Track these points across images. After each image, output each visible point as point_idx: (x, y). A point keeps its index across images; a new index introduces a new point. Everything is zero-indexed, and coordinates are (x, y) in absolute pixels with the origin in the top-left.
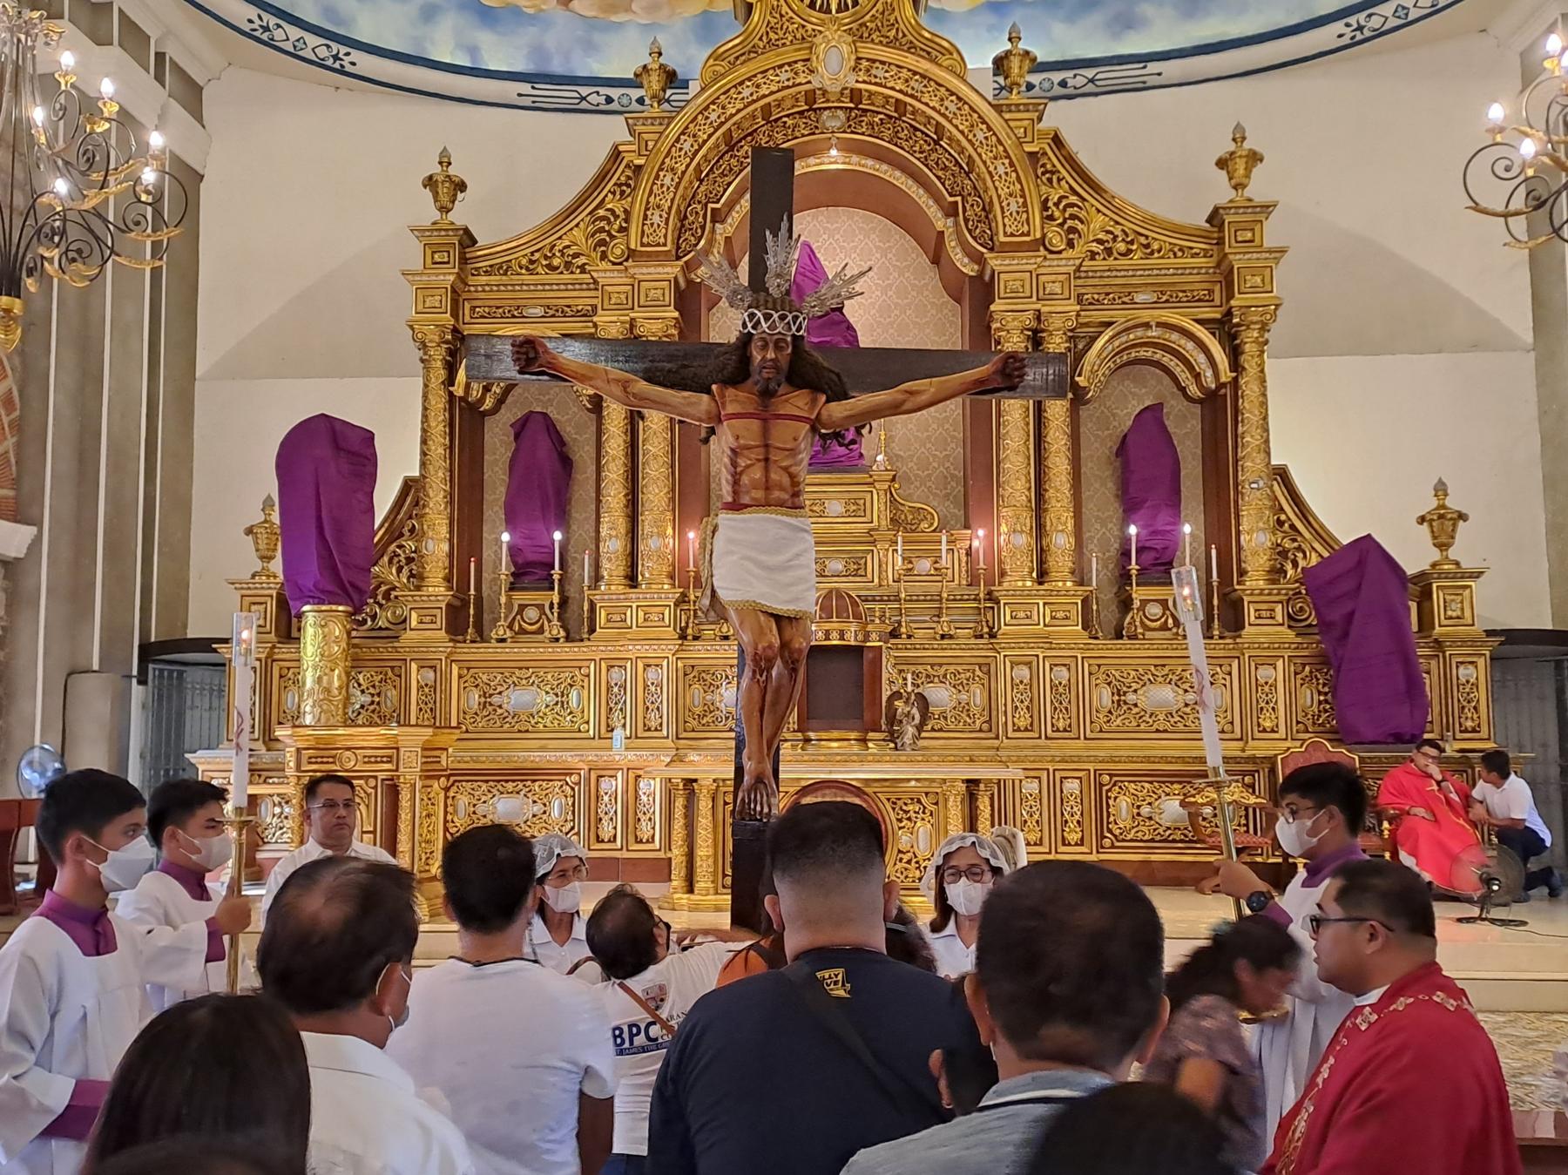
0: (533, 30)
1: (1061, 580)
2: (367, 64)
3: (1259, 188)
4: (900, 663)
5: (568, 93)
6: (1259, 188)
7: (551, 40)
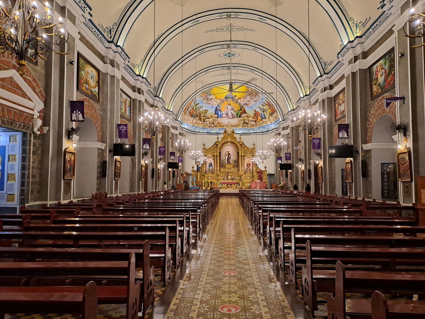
0: (207, 129)
1: (243, 171)
2: (196, 133)
3: (255, 147)
4: (233, 176)
5: (210, 134)
6: (255, 147)
7: (208, 130)
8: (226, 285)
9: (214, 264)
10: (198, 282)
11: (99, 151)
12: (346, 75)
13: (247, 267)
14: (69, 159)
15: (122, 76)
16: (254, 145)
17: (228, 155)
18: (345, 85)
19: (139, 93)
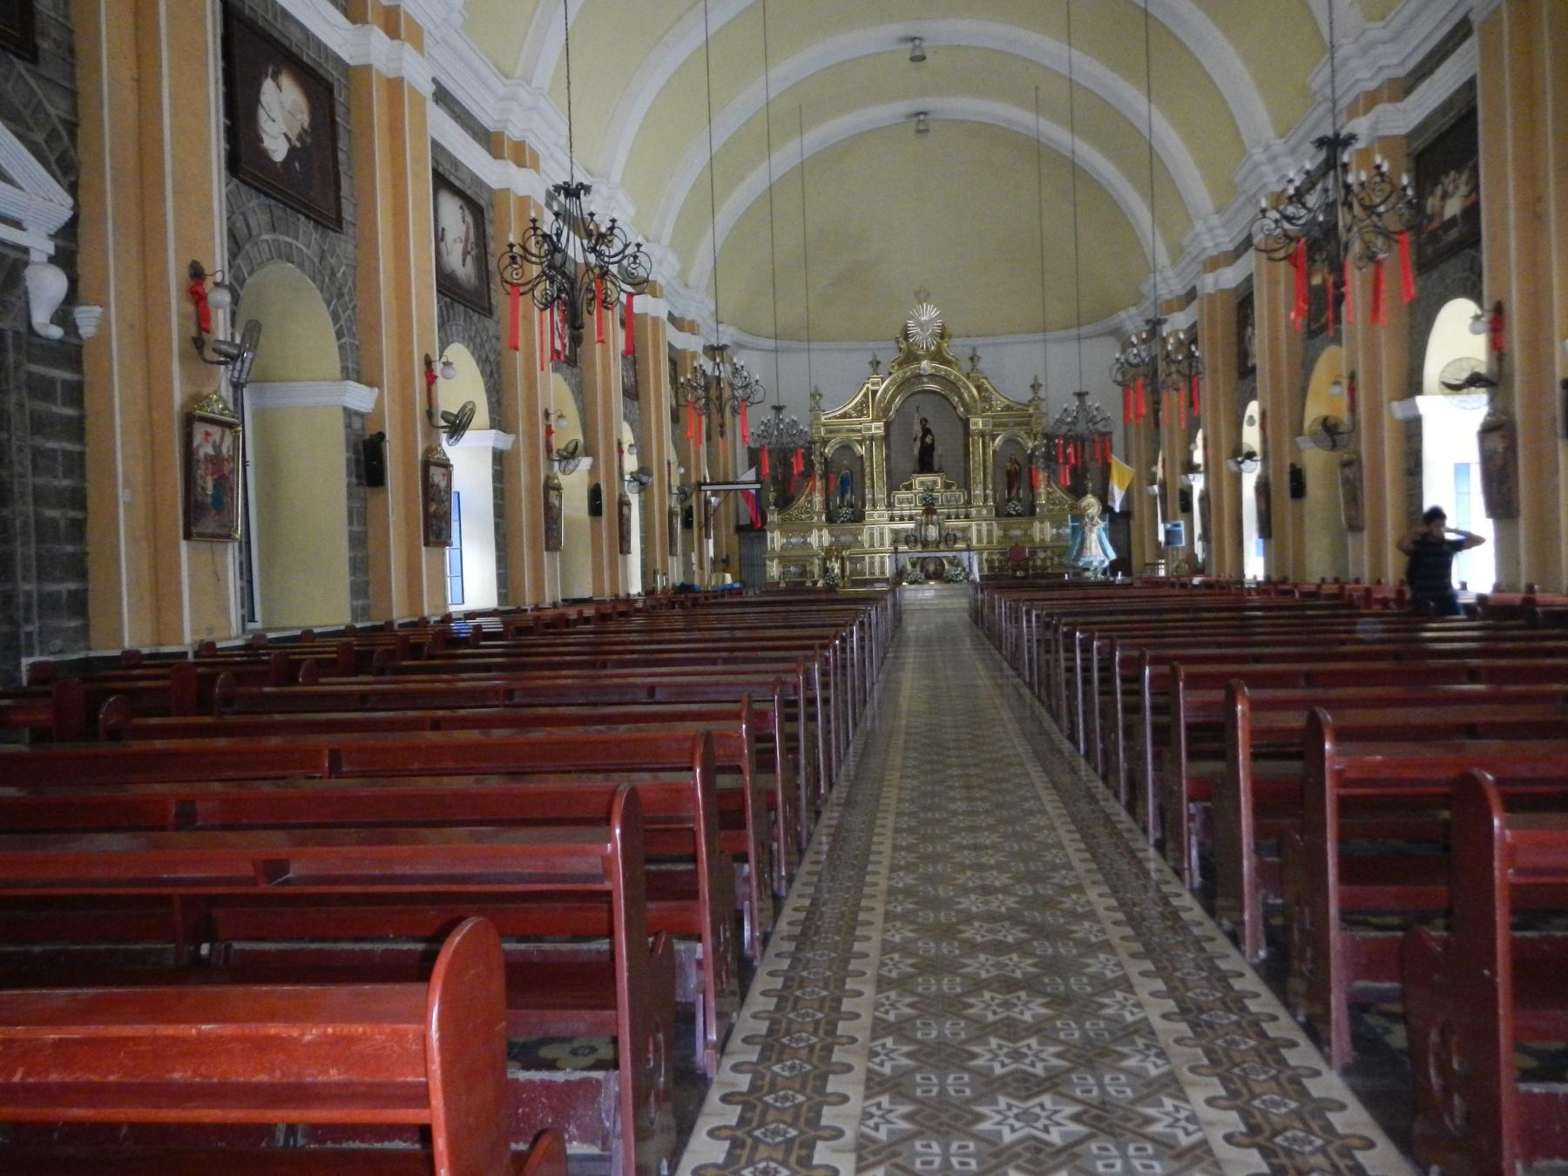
6: (1042, 393)
8: (994, 1042)
9: (906, 917)
10: (833, 1025)
11: (348, 426)
12: (1476, 19)
13: (1083, 929)
14: (210, 451)
15: (434, 80)
16: (1035, 387)
17: (920, 435)
18: (1475, 68)
19: (520, 164)
